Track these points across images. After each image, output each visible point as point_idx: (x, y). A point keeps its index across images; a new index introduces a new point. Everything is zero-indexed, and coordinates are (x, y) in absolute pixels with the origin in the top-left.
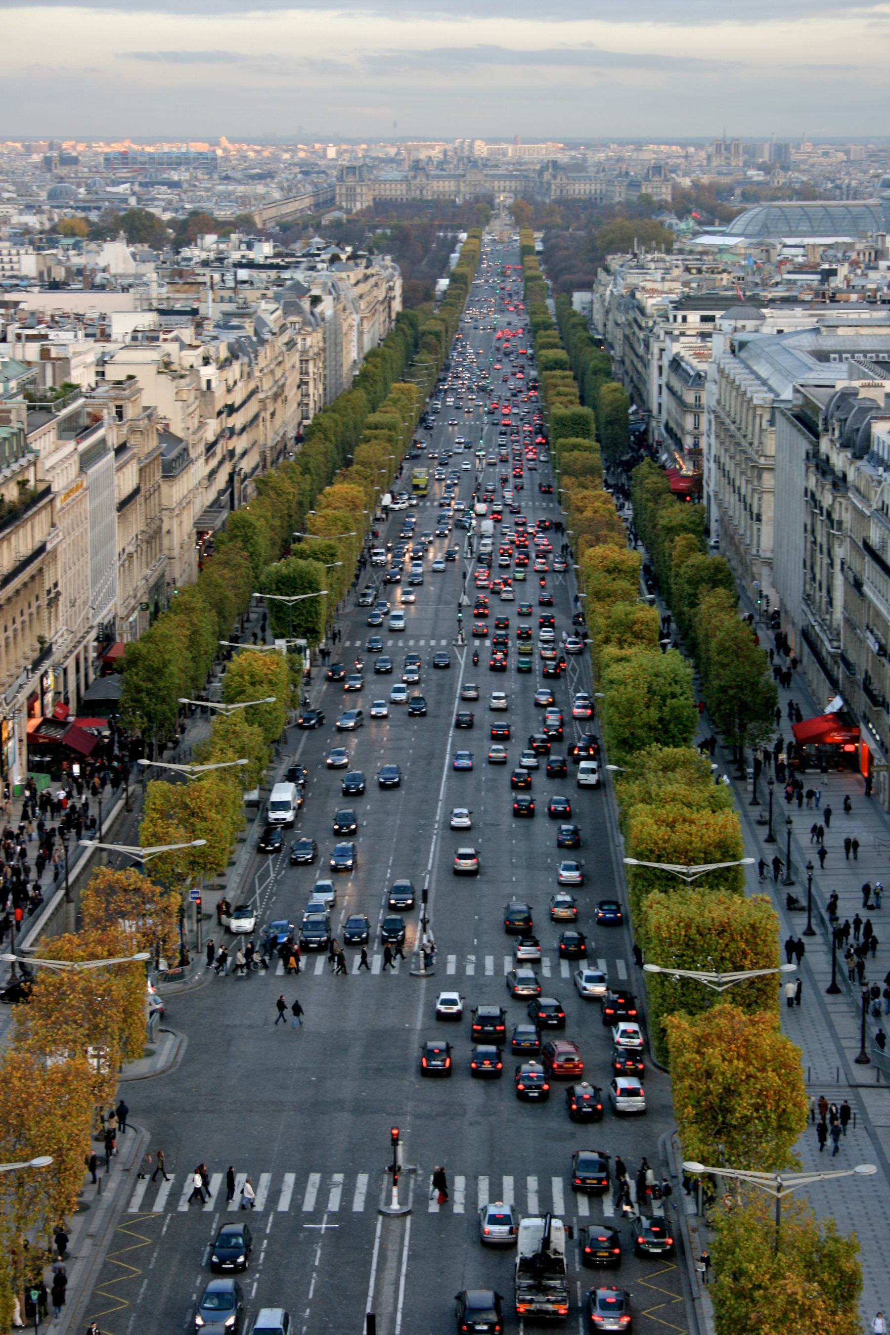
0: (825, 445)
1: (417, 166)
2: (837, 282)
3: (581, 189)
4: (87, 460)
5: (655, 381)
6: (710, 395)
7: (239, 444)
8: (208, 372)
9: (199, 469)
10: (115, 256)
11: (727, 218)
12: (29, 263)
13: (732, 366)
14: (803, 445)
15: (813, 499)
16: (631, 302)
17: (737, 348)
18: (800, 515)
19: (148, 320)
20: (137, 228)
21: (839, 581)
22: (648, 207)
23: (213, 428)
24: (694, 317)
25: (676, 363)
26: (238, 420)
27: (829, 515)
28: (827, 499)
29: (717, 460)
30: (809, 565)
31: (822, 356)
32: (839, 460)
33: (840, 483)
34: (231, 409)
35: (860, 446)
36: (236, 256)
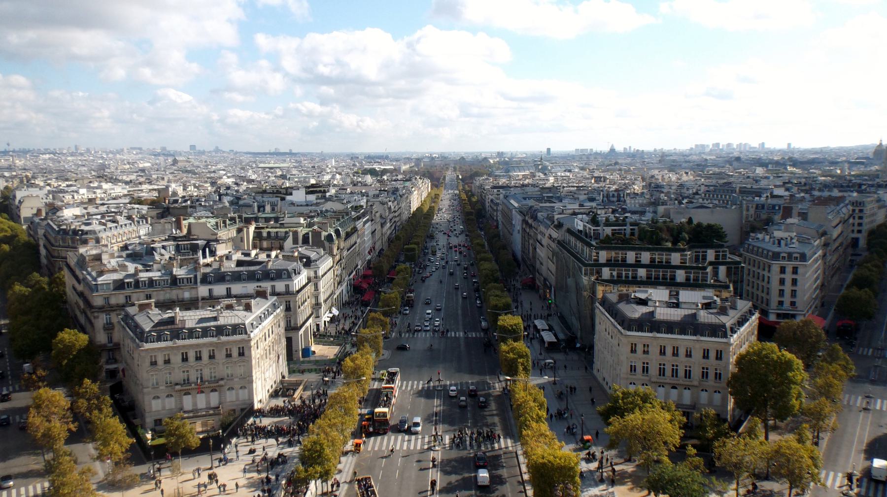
1: (433, 159)
4: (365, 223)
5: (487, 204)
6: (500, 208)
7: (397, 219)
8: (390, 203)
9: (388, 225)
13: (505, 201)
16: (481, 187)
17: (506, 197)
23: (391, 215)
24: (495, 190)
25: (492, 200)
26: (396, 214)
28: (528, 230)
31: (525, 199)
32: (530, 221)
33: (531, 226)
34: (395, 212)
35: (535, 218)
36: (394, 178)
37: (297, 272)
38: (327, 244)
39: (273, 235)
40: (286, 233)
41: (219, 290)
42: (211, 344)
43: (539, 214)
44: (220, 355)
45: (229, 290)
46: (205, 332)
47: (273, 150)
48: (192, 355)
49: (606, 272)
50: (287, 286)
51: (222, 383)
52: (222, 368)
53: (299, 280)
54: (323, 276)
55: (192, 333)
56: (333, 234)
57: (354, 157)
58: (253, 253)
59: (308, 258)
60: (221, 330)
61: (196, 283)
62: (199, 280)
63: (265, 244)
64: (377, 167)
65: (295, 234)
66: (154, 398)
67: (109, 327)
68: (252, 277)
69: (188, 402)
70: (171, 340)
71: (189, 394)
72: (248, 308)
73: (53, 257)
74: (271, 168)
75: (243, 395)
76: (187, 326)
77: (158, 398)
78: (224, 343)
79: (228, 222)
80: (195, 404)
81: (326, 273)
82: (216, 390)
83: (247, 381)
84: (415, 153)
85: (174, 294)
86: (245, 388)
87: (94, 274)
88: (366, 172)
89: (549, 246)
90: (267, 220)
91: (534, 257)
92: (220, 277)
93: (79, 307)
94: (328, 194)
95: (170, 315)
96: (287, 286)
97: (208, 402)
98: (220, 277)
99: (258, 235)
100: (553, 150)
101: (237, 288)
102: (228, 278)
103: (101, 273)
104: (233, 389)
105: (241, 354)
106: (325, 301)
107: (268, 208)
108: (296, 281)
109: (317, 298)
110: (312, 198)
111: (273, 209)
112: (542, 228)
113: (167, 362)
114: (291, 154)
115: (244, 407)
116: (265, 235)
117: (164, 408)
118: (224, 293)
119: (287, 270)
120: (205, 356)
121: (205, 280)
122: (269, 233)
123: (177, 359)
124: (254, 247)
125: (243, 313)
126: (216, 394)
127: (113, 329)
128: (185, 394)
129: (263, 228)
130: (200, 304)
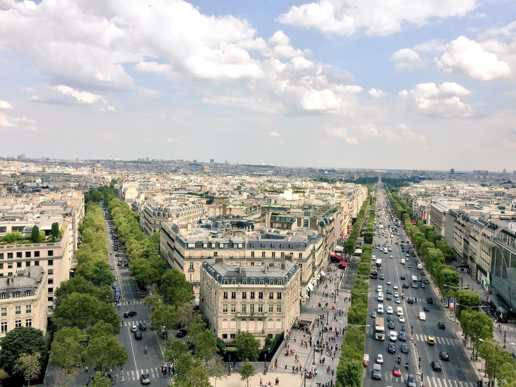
0: (458, 219)
1: (366, 173)
3: (392, 177)
4: (338, 214)
9: (347, 217)
10: (325, 184)
11: (418, 182)
14: (454, 219)
16: (407, 195)
19: (340, 194)
20: (326, 180)
22: (403, 180)
24: (421, 197)
29: (430, 220)
32: (462, 222)
33: (463, 225)
34: (351, 208)
41: (258, 253)
42: (261, 289)
43: (471, 217)
44: (266, 297)
46: (258, 281)
48: (249, 295)
50: (300, 255)
54: (318, 249)
56: (324, 222)
58: (273, 230)
60: (267, 281)
64: (329, 177)
66: (224, 320)
70: (237, 284)
71: (245, 320)
72: (283, 267)
73: (151, 224)
74: (260, 175)
77: (226, 320)
79: (253, 209)
80: (248, 327)
81: (320, 247)
86: (280, 320)
88: (322, 180)
89: (482, 242)
94: (306, 194)
96: (300, 255)
97: (256, 328)
100: (456, 170)
104: (272, 320)
105: (279, 297)
106: (319, 265)
107: (273, 202)
108: (306, 251)
109: (314, 263)
110: (296, 196)
111: (276, 202)
112: (476, 227)
113: (234, 297)
115: (278, 333)
117: (229, 327)
120: (257, 295)
121: (251, 245)
122: (281, 218)
123: (239, 296)
125: (282, 270)
126: (262, 322)
128: (242, 320)
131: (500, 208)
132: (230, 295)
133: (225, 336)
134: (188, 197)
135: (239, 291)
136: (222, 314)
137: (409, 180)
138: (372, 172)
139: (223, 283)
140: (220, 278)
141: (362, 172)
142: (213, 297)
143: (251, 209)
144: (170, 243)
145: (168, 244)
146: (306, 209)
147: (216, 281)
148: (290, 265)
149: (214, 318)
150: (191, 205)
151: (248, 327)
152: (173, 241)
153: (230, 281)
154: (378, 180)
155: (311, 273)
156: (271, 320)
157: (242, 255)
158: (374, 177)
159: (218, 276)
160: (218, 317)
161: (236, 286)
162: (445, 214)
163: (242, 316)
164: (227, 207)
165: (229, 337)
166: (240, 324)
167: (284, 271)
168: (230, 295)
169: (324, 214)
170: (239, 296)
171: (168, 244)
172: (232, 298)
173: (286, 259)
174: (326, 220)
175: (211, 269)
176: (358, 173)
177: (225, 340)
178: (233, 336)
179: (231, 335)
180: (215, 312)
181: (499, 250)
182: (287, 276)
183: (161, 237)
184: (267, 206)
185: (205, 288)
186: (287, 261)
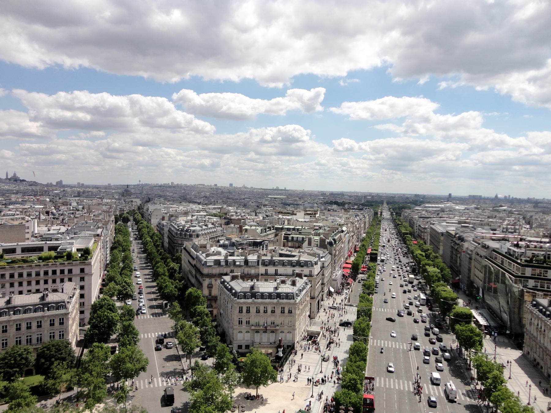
0: (454, 239)
1: (373, 196)
2: (440, 215)
3: (396, 201)
4: (345, 235)
10: (335, 207)
12: (323, 207)
15: (452, 247)
18: (450, 250)
20: (336, 203)
21: (458, 259)
24: (421, 219)
25: (419, 226)
27: (456, 250)
28: (456, 248)
30: (452, 257)
32: (458, 242)
36: (352, 207)
37: (316, 263)
38: (328, 246)
39: (295, 239)
40: (303, 238)
41: (271, 270)
45: (276, 271)
46: (270, 296)
47: (275, 188)
48: (262, 309)
49: (531, 283)
50: (311, 271)
51: (277, 328)
52: (278, 319)
53: (316, 269)
55: (262, 296)
57: (323, 194)
59: (319, 255)
60: (279, 296)
61: (258, 265)
62: (260, 264)
63: (290, 244)
65: (310, 240)
66: (239, 332)
67: (210, 287)
68: (291, 264)
69: (257, 338)
71: (258, 332)
72: (294, 284)
73: (174, 243)
75: (289, 337)
76: (260, 291)
77: (241, 332)
78: (280, 304)
80: (261, 339)
82: (274, 332)
83: (292, 329)
84: (398, 194)
85: (247, 270)
87: (204, 255)
88: (331, 203)
90: (288, 229)
91: (460, 266)
92: (272, 263)
93: (191, 272)
94: (317, 215)
95: (250, 283)
97: (269, 339)
98: (272, 263)
99: (286, 238)
100: (454, 194)
101: (281, 270)
102: (276, 263)
103: (208, 255)
105: (290, 312)
107: (286, 222)
109: (323, 279)
111: (289, 224)
114: (285, 190)
116: (290, 238)
117: (244, 339)
118: (274, 272)
119: (311, 262)
121: (264, 264)
122: (293, 238)
124: (284, 246)
125: (293, 287)
127: (212, 287)
128: (256, 332)
129: (289, 234)
130: (260, 277)
131: (493, 230)
132: (244, 310)
133: (240, 347)
134: (209, 218)
135: (253, 305)
136: (237, 327)
137: (411, 203)
138: (378, 195)
139: (238, 298)
140: (236, 292)
141: (370, 196)
142: (229, 311)
143: (265, 229)
144: (191, 260)
145: (189, 261)
146: (316, 229)
147: (232, 297)
148: (300, 282)
149: (230, 330)
150: (210, 226)
151: (261, 339)
152: (193, 259)
153: (245, 297)
154: (383, 204)
155: (320, 289)
156: (282, 332)
157: (257, 272)
158: (379, 200)
159: (234, 291)
160: (234, 329)
161: (250, 301)
162: (442, 234)
163: (256, 328)
164: (244, 228)
165: (244, 347)
166: (254, 336)
167: (294, 287)
168: (244, 310)
169: (333, 234)
170: (253, 310)
171: (189, 261)
172: (247, 312)
173: (296, 277)
174: (334, 240)
175: (228, 285)
176: (365, 197)
177: (240, 350)
178: (247, 347)
179: (246, 346)
180: (231, 325)
181: (489, 267)
182: (297, 292)
183: (183, 255)
184: (281, 227)
185: (222, 302)
186: (297, 278)
